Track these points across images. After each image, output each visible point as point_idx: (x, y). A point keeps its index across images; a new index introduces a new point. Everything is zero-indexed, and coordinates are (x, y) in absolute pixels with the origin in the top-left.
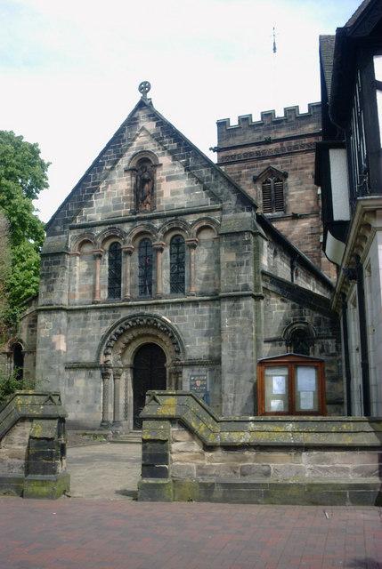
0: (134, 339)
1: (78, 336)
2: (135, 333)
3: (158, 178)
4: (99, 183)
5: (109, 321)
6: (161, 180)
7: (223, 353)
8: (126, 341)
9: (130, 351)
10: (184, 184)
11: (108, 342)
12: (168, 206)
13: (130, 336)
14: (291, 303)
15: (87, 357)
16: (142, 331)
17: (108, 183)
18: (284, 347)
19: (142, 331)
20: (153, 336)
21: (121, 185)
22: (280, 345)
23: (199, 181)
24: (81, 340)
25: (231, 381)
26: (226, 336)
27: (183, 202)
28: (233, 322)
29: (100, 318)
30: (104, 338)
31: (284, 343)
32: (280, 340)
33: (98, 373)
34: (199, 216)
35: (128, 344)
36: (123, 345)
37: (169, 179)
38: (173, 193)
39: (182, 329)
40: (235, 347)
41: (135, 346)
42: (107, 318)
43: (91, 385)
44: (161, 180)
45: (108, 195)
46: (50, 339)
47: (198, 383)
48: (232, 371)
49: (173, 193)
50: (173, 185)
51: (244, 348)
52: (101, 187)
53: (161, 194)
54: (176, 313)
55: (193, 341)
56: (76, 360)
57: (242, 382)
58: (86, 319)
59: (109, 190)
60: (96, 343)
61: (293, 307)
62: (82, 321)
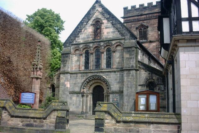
0: (93, 84)
2: (93, 82)
3: (102, 28)
4: (82, 29)
5: (85, 77)
6: (104, 28)
7: (124, 89)
8: (90, 84)
10: (111, 30)
15: (77, 89)
16: (96, 81)
17: (85, 29)
18: (145, 88)
19: (96, 81)
20: (100, 83)
21: (89, 30)
22: (144, 87)
23: (117, 29)
25: (127, 99)
26: (125, 84)
27: (111, 36)
29: (82, 76)
31: (145, 86)
34: (116, 41)
35: (91, 85)
37: (106, 28)
38: (107, 33)
40: (128, 87)
41: (93, 86)
43: (78, 99)
44: (104, 28)
45: (85, 33)
46: (64, 83)
47: (115, 99)
48: (127, 95)
49: (107, 33)
50: (108, 30)
51: (131, 88)
52: (83, 30)
53: (103, 33)
54: (108, 75)
55: (114, 85)
56: (73, 90)
57: (131, 99)
58: (77, 76)
59: (85, 32)
60: (80, 85)
61: (149, 74)
62: (75, 77)
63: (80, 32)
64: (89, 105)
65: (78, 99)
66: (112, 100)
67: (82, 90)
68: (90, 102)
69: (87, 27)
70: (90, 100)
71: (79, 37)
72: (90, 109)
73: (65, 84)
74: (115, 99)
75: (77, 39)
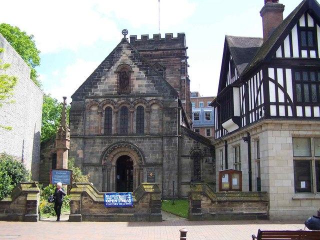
1: (90, 151)
2: (118, 150)
3: (132, 78)
4: (101, 77)
6: (134, 79)
9: (115, 159)
10: (145, 82)
11: (105, 155)
12: (137, 92)
13: (116, 152)
14: (193, 141)
15: (95, 161)
17: (106, 78)
18: (190, 160)
21: (112, 79)
22: (188, 159)
23: (153, 81)
24: (92, 153)
25: (167, 174)
26: (166, 154)
27: (144, 90)
28: (168, 148)
30: (104, 152)
32: (188, 156)
33: (100, 169)
34: (152, 98)
36: (112, 156)
37: (137, 79)
38: (139, 86)
39: (143, 150)
40: (169, 159)
42: (105, 143)
43: (97, 175)
44: (134, 79)
45: (106, 83)
46: (76, 152)
47: (151, 174)
48: (168, 169)
49: (139, 86)
50: (140, 82)
51: (173, 160)
52: (102, 79)
53: (134, 86)
54: (140, 142)
56: (89, 162)
57: (172, 175)
58: (94, 143)
59: (106, 81)
60: (100, 155)
61: (194, 142)
63: (98, 80)
64: (111, 182)
65: (97, 175)
66: (146, 175)
67: (103, 162)
68: (113, 178)
69: (109, 74)
70: (113, 176)
71: (97, 87)
72: (113, 187)
73: (78, 153)
74: (151, 174)
75: (93, 90)
